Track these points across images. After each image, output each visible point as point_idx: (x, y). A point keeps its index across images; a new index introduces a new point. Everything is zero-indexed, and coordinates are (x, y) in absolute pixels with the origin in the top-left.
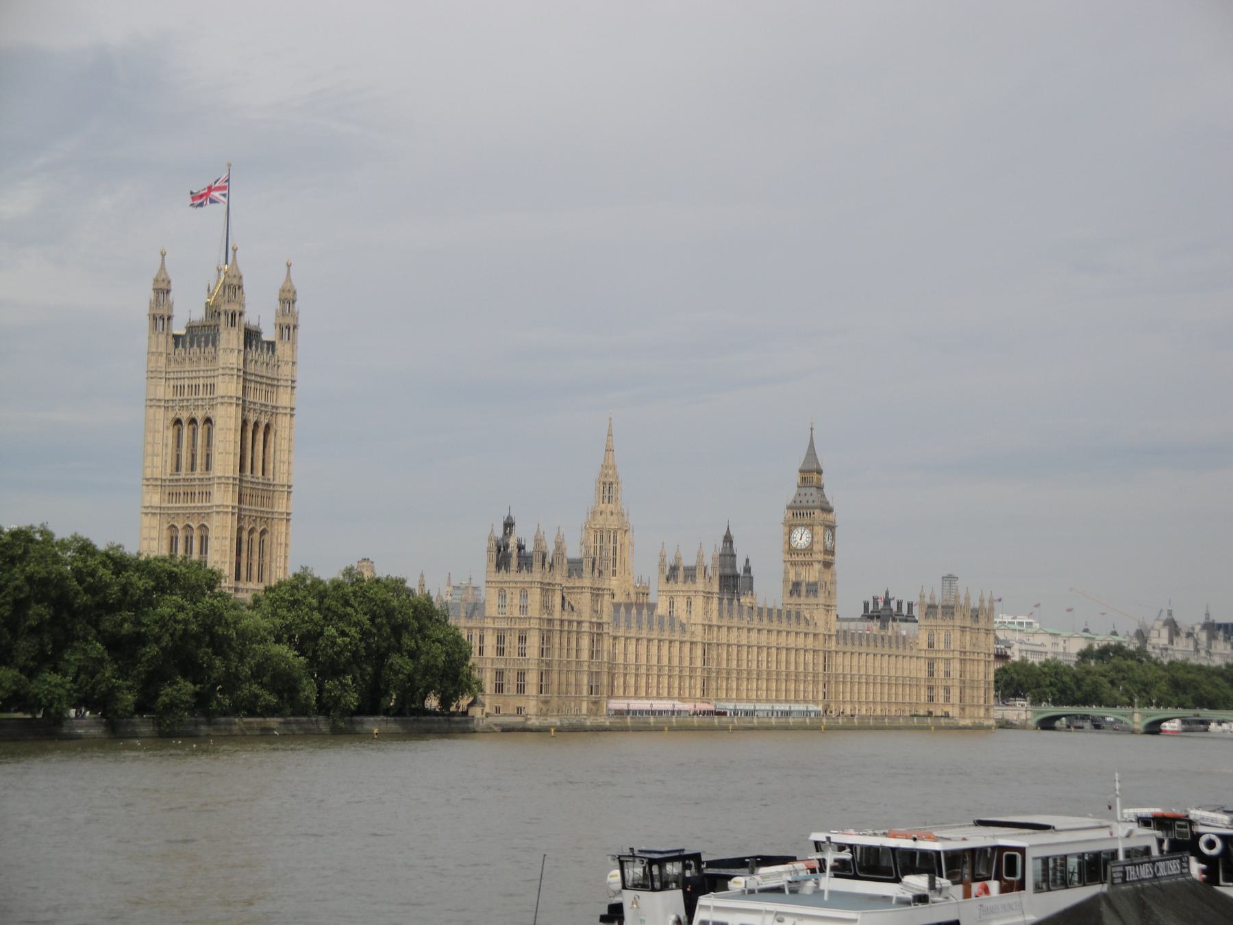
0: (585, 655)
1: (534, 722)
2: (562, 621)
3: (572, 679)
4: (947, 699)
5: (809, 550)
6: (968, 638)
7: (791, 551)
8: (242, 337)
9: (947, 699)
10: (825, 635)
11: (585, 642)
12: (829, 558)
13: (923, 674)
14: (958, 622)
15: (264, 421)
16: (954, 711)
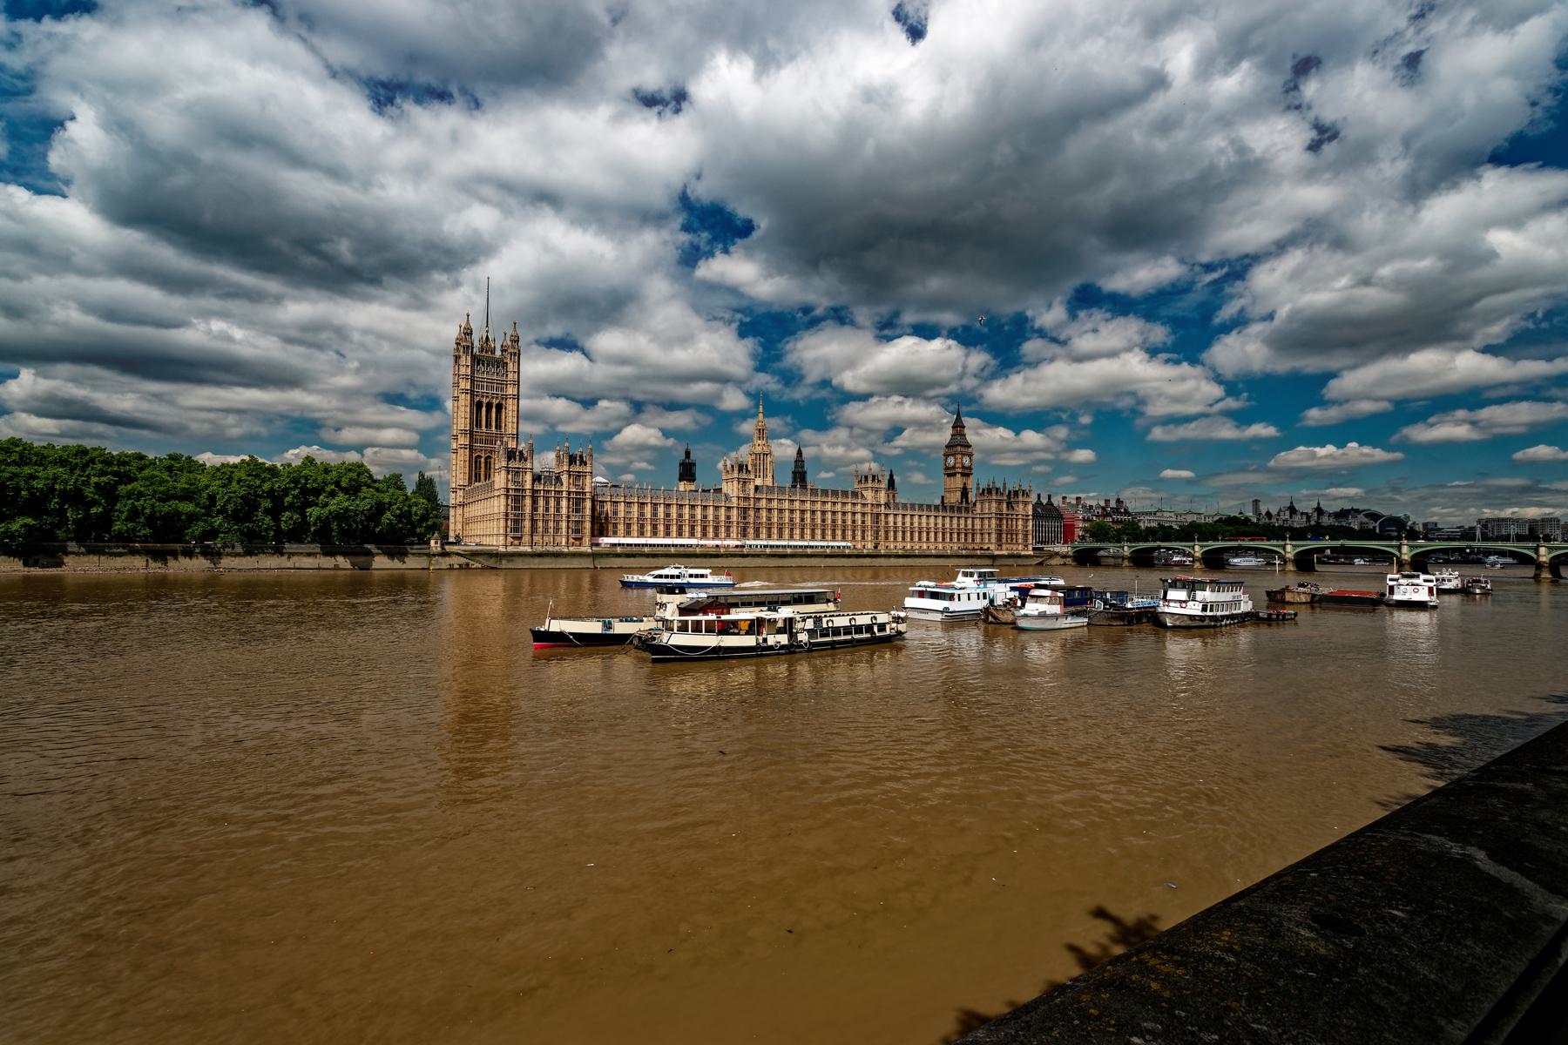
0: (564, 511)
1: (502, 549)
2: (534, 491)
3: (551, 524)
4: (989, 540)
5: (954, 468)
6: (1005, 505)
7: (947, 468)
8: (469, 358)
9: (989, 540)
10: (872, 505)
11: (564, 503)
12: (966, 471)
13: (978, 527)
14: (994, 497)
15: (495, 402)
16: (992, 547)
